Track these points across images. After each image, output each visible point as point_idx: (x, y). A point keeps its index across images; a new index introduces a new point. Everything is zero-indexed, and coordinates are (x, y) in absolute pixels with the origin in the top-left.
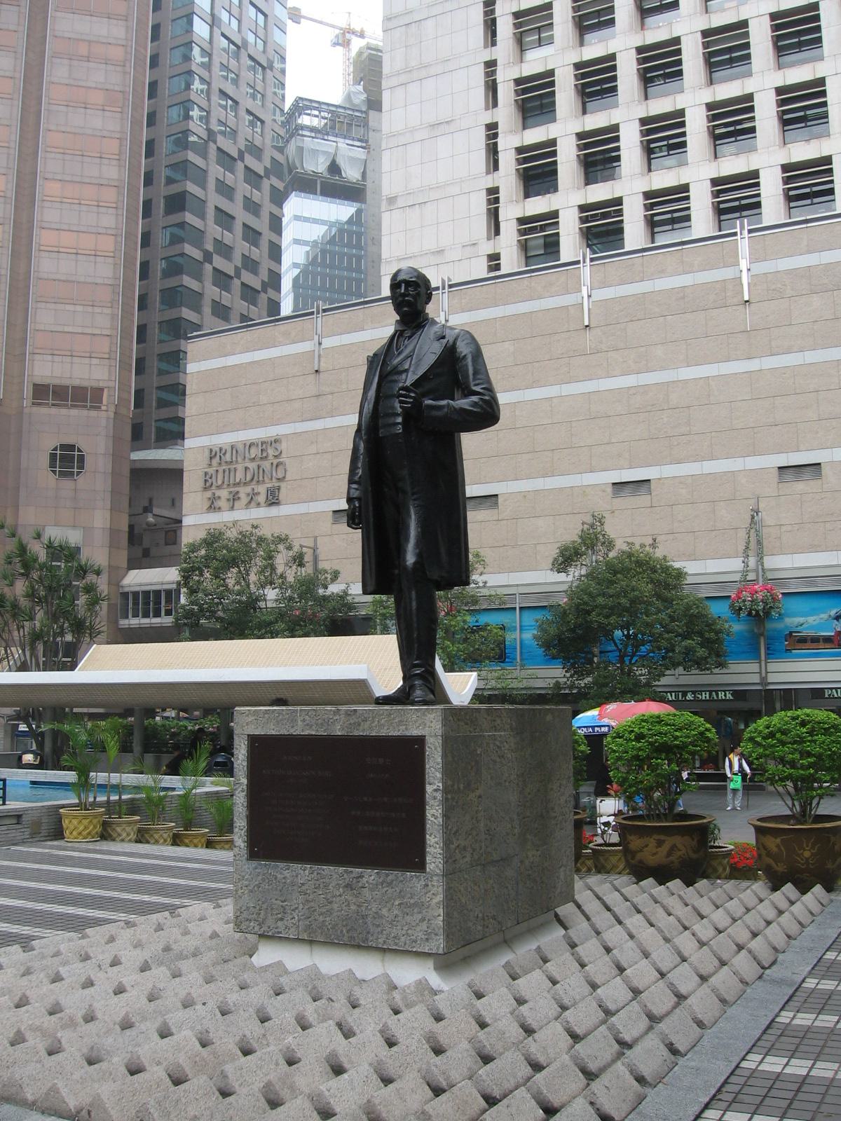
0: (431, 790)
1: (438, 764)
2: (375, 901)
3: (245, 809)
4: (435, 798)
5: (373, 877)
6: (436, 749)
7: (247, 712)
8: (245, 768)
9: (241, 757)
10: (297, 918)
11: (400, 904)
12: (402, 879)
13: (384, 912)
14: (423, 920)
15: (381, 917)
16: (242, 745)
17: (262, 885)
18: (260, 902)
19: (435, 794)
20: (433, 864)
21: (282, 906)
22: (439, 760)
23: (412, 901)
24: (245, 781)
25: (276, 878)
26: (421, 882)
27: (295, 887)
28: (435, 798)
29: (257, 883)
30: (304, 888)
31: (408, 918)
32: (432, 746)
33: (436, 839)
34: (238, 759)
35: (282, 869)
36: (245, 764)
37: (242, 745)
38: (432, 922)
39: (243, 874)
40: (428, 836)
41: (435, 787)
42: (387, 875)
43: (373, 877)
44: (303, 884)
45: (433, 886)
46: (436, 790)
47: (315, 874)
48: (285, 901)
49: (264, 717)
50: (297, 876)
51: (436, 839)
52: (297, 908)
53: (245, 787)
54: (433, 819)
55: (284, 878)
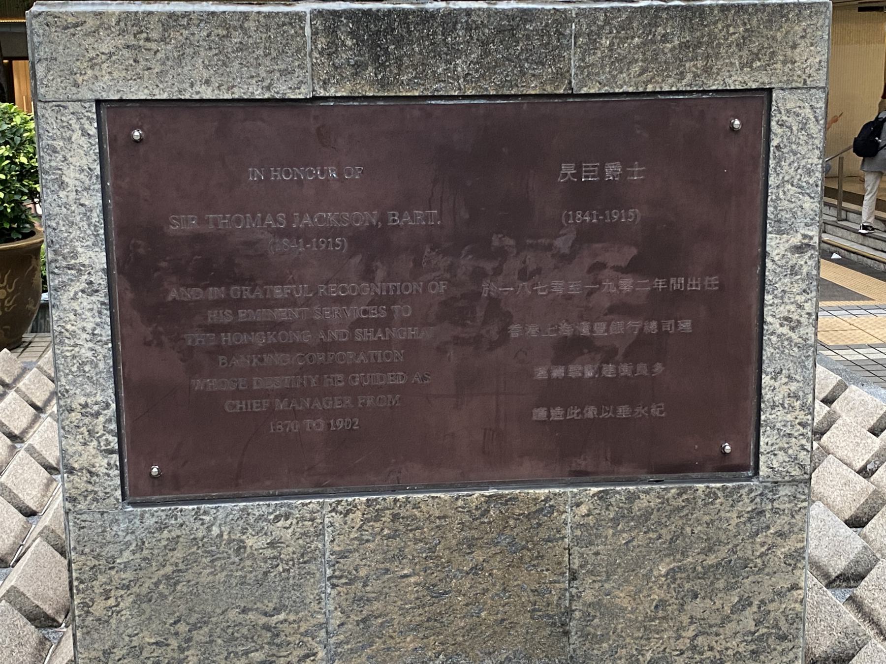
0: (782, 250)
1: (809, 172)
2: (591, 573)
3: (105, 350)
4: (794, 271)
5: (583, 509)
6: (803, 127)
7: (91, 23)
8: (96, 216)
9: (71, 177)
10: (321, 654)
11: (671, 574)
12: (680, 502)
13: (622, 599)
14: (745, 603)
15: (612, 613)
16: (76, 136)
17: (189, 575)
18: (182, 628)
19: (794, 259)
20: (781, 456)
21: (267, 628)
22: (815, 160)
23: (712, 560)
24: (100, 259)
25: (241, 547)
26: (739, 507)
27: (312, 567)
28: (794, 271)
29: (169, 569)
30: (347, 564)
31: (696, 607)
32: (791, 120)
33: (794, 386)
34: (62, 185)
35: (260, 518)
36: (95, 200)
37: (76, 136)
38: (771, 607)
39: (110, 550)
40: (766, 380)
41: (796, 240)
42: (632, 498)
43: (583, 509)
44: (343, 555)
45: (776, 512)
46: (799, 249)
47: (387, 517)
48: (277, 611)
49: (163, 40)
50: (320, 534)
51: (794, 386)
52: (320, 626)
53: (100, 280)
54: (785, 330)
55: (271, 544)
